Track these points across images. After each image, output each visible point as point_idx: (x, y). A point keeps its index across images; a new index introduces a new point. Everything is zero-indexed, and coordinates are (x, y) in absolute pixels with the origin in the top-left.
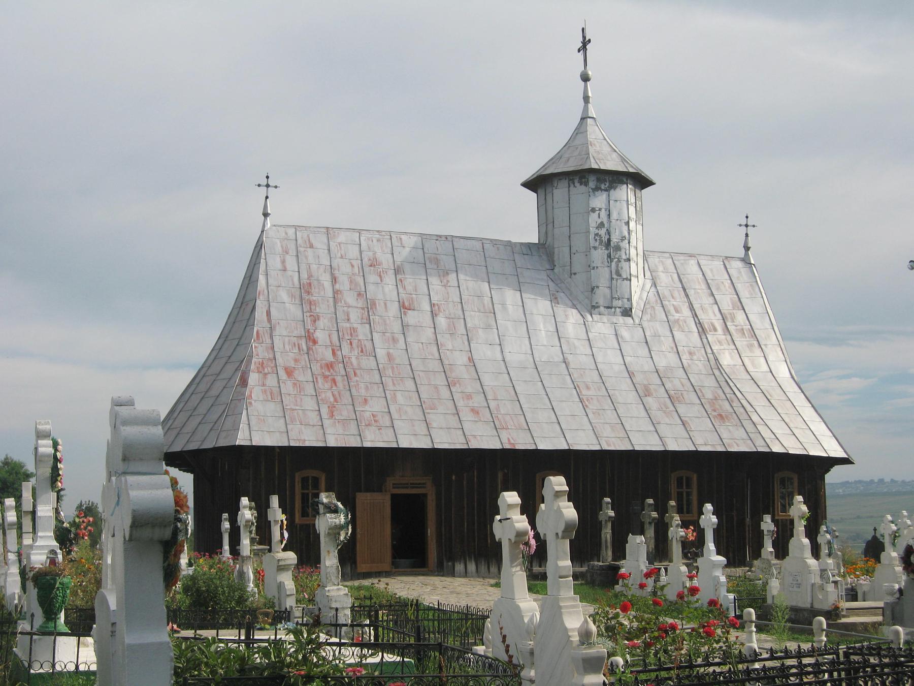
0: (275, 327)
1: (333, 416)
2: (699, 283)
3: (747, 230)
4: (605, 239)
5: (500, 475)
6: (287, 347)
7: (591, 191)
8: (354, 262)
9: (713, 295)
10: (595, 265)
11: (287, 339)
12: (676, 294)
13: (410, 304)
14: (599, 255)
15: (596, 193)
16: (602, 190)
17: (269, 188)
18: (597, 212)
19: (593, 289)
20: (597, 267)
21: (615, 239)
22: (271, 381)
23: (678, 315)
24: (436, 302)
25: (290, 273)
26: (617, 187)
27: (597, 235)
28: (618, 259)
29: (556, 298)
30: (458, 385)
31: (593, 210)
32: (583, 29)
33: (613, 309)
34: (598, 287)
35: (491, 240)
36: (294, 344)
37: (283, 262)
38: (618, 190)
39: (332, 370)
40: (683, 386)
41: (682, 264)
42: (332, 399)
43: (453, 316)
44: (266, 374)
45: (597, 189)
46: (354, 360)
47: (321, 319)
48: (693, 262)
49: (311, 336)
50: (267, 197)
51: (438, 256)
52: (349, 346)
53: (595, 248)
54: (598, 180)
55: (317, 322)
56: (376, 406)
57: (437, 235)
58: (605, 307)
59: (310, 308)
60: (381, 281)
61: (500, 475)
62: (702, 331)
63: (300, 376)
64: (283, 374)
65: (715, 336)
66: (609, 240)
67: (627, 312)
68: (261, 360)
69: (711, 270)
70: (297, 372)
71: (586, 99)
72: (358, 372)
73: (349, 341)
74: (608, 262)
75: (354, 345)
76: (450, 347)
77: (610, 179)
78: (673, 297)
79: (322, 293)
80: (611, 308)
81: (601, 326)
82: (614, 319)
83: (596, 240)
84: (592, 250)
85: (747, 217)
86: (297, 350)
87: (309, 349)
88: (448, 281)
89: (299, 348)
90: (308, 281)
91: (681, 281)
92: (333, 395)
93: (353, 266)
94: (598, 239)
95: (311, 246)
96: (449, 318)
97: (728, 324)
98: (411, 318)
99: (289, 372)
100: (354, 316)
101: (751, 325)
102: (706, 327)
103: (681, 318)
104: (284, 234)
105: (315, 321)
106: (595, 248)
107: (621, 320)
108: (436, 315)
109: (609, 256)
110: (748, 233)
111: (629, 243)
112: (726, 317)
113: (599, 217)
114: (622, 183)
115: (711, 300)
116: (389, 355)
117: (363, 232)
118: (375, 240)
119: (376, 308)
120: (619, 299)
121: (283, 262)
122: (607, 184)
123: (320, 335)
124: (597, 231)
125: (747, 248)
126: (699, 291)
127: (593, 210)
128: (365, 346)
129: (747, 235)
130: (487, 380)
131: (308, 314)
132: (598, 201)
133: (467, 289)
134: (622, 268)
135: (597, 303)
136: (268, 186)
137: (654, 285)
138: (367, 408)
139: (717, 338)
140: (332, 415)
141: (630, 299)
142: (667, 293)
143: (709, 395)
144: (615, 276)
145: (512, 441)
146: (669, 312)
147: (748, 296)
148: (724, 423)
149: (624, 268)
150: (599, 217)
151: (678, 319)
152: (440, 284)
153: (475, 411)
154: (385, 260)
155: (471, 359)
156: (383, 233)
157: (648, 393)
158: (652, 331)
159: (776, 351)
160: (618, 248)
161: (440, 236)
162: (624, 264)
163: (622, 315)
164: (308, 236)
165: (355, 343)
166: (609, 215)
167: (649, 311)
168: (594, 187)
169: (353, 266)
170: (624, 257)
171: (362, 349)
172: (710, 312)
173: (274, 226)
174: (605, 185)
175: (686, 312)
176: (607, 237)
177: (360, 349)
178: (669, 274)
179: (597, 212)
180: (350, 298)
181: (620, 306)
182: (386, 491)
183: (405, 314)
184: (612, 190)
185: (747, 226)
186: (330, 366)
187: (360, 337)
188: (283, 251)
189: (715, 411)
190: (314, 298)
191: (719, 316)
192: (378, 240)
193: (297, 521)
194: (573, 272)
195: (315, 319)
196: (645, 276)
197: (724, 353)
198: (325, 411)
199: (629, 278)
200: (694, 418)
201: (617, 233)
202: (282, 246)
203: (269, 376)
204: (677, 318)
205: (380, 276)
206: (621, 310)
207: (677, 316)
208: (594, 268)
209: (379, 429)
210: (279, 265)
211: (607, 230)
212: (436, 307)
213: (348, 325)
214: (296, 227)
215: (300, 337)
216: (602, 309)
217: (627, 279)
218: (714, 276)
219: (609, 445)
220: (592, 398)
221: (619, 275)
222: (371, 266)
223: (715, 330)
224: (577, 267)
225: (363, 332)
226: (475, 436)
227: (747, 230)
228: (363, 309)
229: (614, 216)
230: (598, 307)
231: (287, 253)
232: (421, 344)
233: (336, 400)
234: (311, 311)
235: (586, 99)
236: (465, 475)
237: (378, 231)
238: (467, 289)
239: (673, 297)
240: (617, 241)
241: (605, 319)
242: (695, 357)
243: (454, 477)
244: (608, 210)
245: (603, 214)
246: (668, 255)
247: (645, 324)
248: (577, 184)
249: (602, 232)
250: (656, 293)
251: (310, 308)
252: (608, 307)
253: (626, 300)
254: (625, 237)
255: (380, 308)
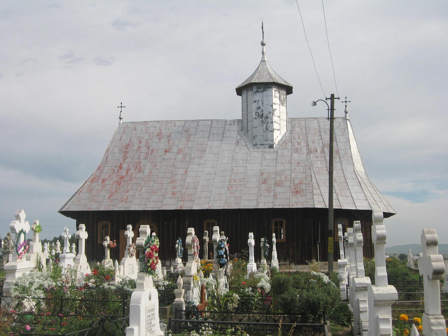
0: (107, 163)
1: (110, 197)
2: (316, 130)
3: (346, 104)
4: (261, 114)
5: (187, 222)
6: (109, 171)
7: (254, 93)
8: (151, 135)
9: (321, 136)
10: (255, 126)
11: (110, 168)
12: (301, 137)
13: (168, 150)
14: (257, 122)
15: (257, 94)
16: (259, 92)
17: (122, 108)
18: (257, 102)
19: (254, 137)
20: (257, 127)
21: (265, 114)
22: (94, 185)
23: (298, 146)
24: (180, 148)
25: (122, 141)
26: (267, 90)
27: (256, 112)
28: (267, 122)
29: (238, 143)
30: (173, 183)
31: (255, 102)
32: (262, 23)
33: (264, 146)
34: (257, 136)
35: (217, 120)
36: (112, 169)
37: (121, 137)
38: (267, 91)
39: (122, 179)
40: (286, 178)
41: (309, 122)
42: (114, 191)
43: (186, 154)
44: (94, 182)
45: (257, 92)
46: (134, 175)
47: (128, 158)
48: (316, 121)
49: (121, 166)
50: (121, 111)
51: (189, 129)
52: (135, 169)
53: (256, 118)
54: (258, 88)
55: (126, 160)
56: (131, 193)
57: (192, 120)
58: (260, 145)
59: (125, 154)
60: (160, 141)
61: (187, 222)
62: (309, 152)
63: (106, 183)
64: (100, 181)
65: (315, 155)
66: (263, 114)
67: (271, 146)
68: (95, 177)
69: (325, 124)
70: (107, 181)
71: (263, 53)
72: (132, 179)
73: (135, 167)
74: (262, 124)
75: (137, 168)
76: (179, 167)
77: (264, 87)
78: (299, 138)
79: (132, 148)
80: (263, 145)
81: (256, 154)
82: (264, 150)
83: (256, 115)
84: (255, 119)
85: (346, 98)
86: (112, 172)
87: (118, 171)
88: (190, 139)
89: (113, 172)
90: (128, 144)
91: (306, 130)
92: (116, 189)
93: (150, 136)
94: (257, 114)
95: (135, 129)
96: (184, 155)
97: (325, 148)
98: (168, 155)
99: (104, 181)
100: (142, 156)
101: (338, 148)
102: (312, 150)
103: (300, 147)
104: (126, 126)
105: (125, 160)
106: (256, 118)
107: (268, 150)
108: (178, 154)
109: (262, 121)
110: (347, 105)
111: (273, 115)
112: (325, 145)
113: (258, 104)
114: (269, 87)
115: (319, 138)
116: (150, 172)
117: (160, 122)
118: (164, 125)
119: (153, 153)
120: (267, 141)
121: (121, 137)
122: (262, 89)
123: (125, 166)
124: (257, 111)
125: (346, 112)
126: (314, 134)
127: (255, 102)
128: (142, 168)
129: (346, 106)
130: (188, 180)
131: (123, 157)
132: (258, 96)
133: (197, 141)
134: (269, 126)
135: (256, 143)
136: (121, 107)
137: (291, 133)
138: (127, 194)
139: (316, 155)
140: (109, 197)
141: (272, 140)
142: (296, 136)
143: (297, 182)
144: (265, 130)
145: (182, 206)
146: (294, 145)
147: (341, 134)
148: (297, 195)
149: (270, 126)
150: (258, 104)
151: (298, 148)
152: (185, 140)
153: (174, 194)
154: (164, 132)
155: (186, 172)
156: (169, 121)
157: (265, 182)
158: (282, 154)
159: (349, 160)
160: (267, 118)
161: (193, 120)
162: (269, 124)
163: (269, 148)
164: (136, 126)
165: (138, 167)
166: (263, 103)
167: (284, 145)
168: (255, 91)
169: (150, 136)
170: (270, 121)
171: (140, 170)
172: (317, 145)
173: (124, 123)
174: (261, 89)
175: (303, 144)
176: (262, 113)
177: (139, 170)
178: (301, 128)
179: (257, 102)
180: (144, 149)
181: (268, 144)
182: (136, 230)
183: (165, 154)
184: (265, 92)
185: (346, 102)
186: (122, 178)
187: (141, 165)
188: (123, 132)
189: (295, 189)
190: (128, 150)
191: (321, 145)
192: (165, 125)
193: (99, 242)
194: (248, 130)
195: (125, 158)
196: (287, 130)
197: (317, 162)
198: (108, 195)
199: (272, 130)
200: (281, 193)
201: (267, 111)
202: (123, 131)
203: (94, 183)
204: (298, 147)
205: (160, 139)
206: (268, 145)
207: (297, 146)
208: (255, 128)
209: (126, 203)
210: (119, 138)
211: (262, 110)
212: (180, 150)
213: (138, 160)
214: (132, 122)
215: (116, 167)
216: (259, 146)
217: (271, 131)
218: (325, 127)
219: (228, 206)
220: (234, 186)
221: (267, 129)
222: (158, 135)
223: (317, 151)
224: (249, 129)
225: (143, 162)
226: (166, 205)
227: (346, 104)
228: (147, 153)
229: (265, 103)
230: (257, 145)
231: (124, 133)
232: (166, 166)
233: (115, 192)
234: (125, 156)
235: (263, 53)
236: (171, 222)
237: (166, 121)
238: (197, 141)
239: (299, 138)
240: (267, 114)
241: (259, 150)
242: (300, 165)
243: (166, 223)
244: (262, 101)
245: (260, 103)
246: (304, 119)
247: (279, 151)
248: (249, 91)
249: (259, 111)
250: (290, 137)
251: (125, 154)
252: (262, 145)
253: (271, 141)
254: (271, 112)
255: (154, 153)
